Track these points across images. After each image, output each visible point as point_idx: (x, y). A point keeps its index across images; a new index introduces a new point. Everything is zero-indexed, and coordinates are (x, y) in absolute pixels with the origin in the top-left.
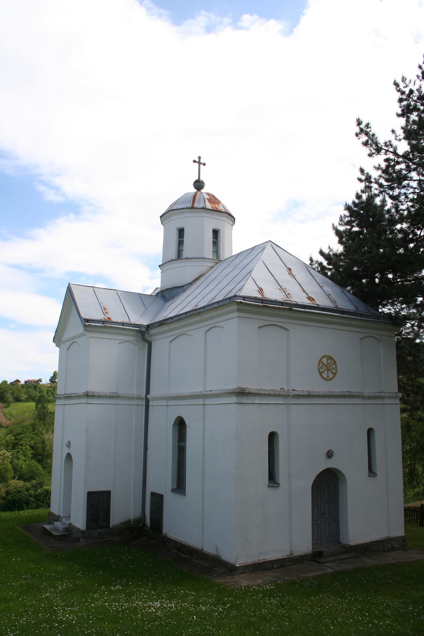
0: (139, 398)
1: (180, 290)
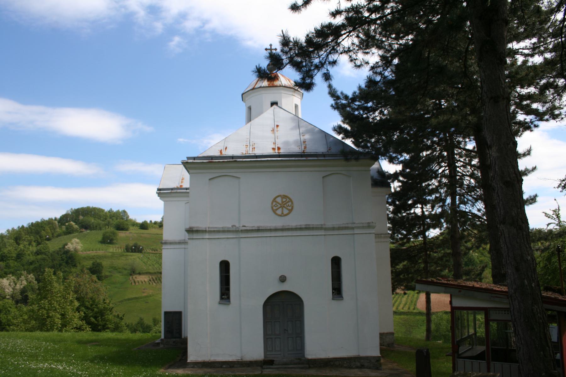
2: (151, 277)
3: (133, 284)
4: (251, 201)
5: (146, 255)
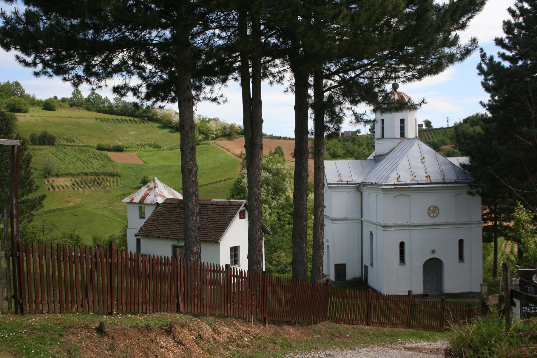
0: (358, 219)
1: (382, 157)
2: (73, 180)
3: (52, 190)
4: (416, 209)
5: (61, 148)
